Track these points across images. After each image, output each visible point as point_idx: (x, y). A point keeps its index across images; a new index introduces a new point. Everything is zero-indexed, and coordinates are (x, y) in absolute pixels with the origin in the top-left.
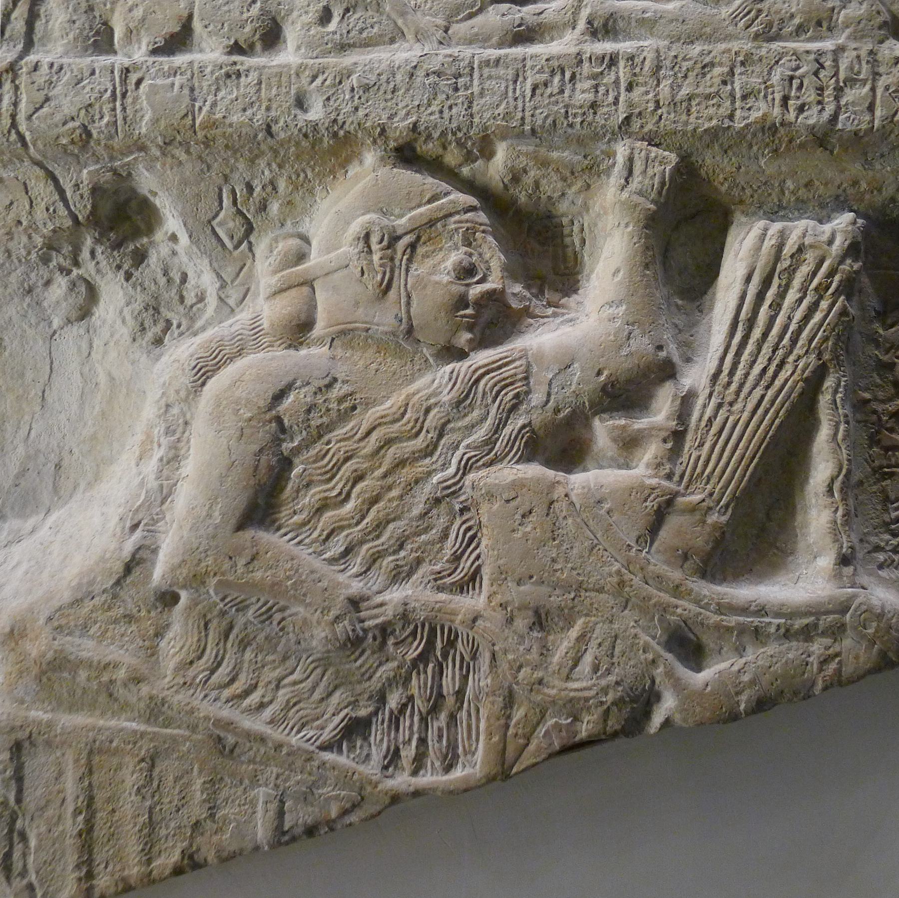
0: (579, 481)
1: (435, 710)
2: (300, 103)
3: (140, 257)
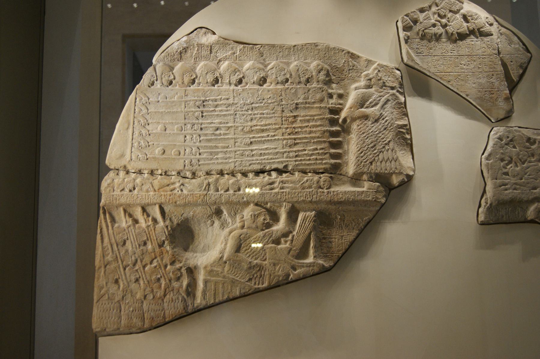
0: (279, 246)
1: (261, 277)
2: (243, 198)
3: (221, 217)
